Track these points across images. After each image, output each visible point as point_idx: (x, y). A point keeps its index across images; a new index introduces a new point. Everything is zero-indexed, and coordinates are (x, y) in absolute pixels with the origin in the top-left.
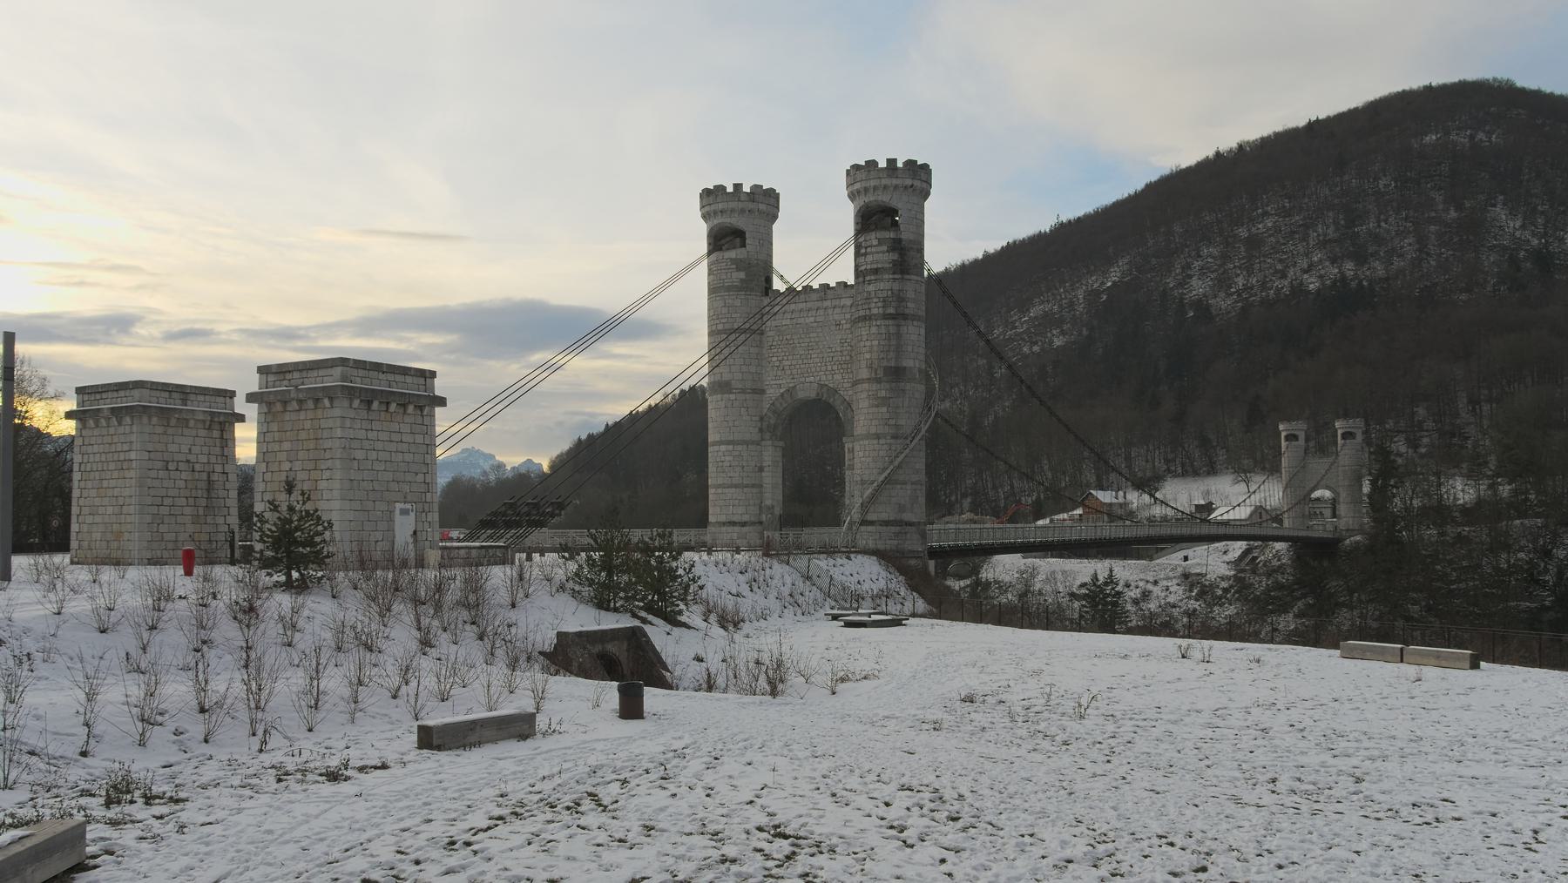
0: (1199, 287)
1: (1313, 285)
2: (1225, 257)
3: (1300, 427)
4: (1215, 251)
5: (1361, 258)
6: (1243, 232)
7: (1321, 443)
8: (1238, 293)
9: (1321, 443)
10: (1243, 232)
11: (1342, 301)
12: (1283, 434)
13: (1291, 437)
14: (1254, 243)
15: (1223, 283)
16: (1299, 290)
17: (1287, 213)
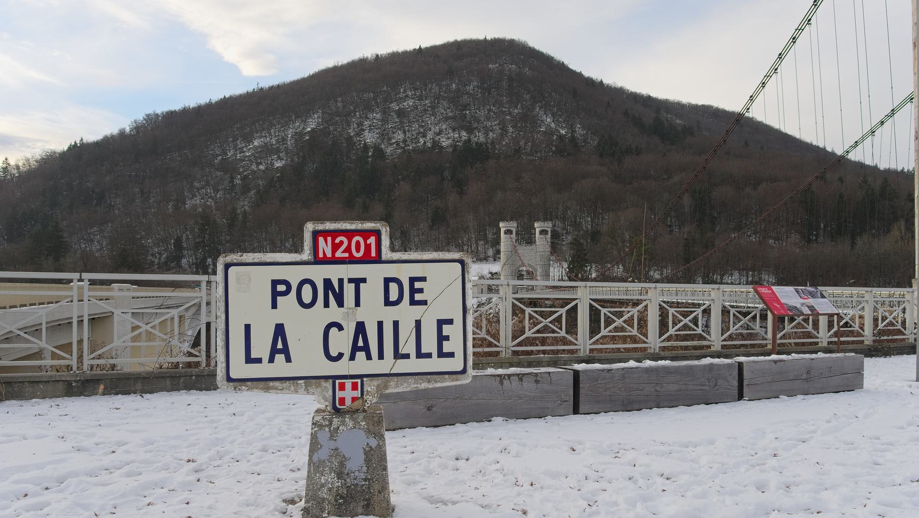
0: (370, 138)
1: (445, 142)
2: (385, 121)
3: (513, 225)
4: (378, 116)
5: (470, 130)
6: (395, 106)
7: (525, 236)
8: (397, 143)
9: (525, 236)
10: (395, 106)
11: (470, 155)
12: (502, 230)
13: (508, 232)
14: (401, 113)
15: (384, 136)
16: (436, 144)
17: (420, 98)
